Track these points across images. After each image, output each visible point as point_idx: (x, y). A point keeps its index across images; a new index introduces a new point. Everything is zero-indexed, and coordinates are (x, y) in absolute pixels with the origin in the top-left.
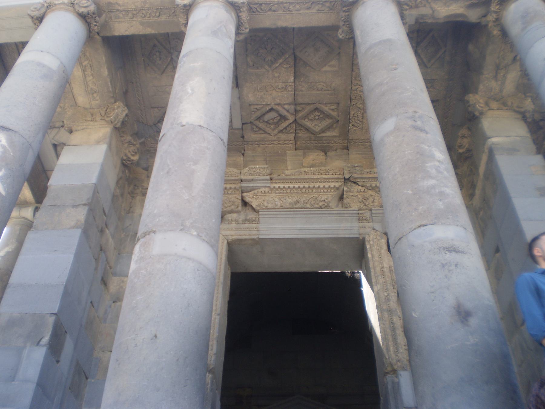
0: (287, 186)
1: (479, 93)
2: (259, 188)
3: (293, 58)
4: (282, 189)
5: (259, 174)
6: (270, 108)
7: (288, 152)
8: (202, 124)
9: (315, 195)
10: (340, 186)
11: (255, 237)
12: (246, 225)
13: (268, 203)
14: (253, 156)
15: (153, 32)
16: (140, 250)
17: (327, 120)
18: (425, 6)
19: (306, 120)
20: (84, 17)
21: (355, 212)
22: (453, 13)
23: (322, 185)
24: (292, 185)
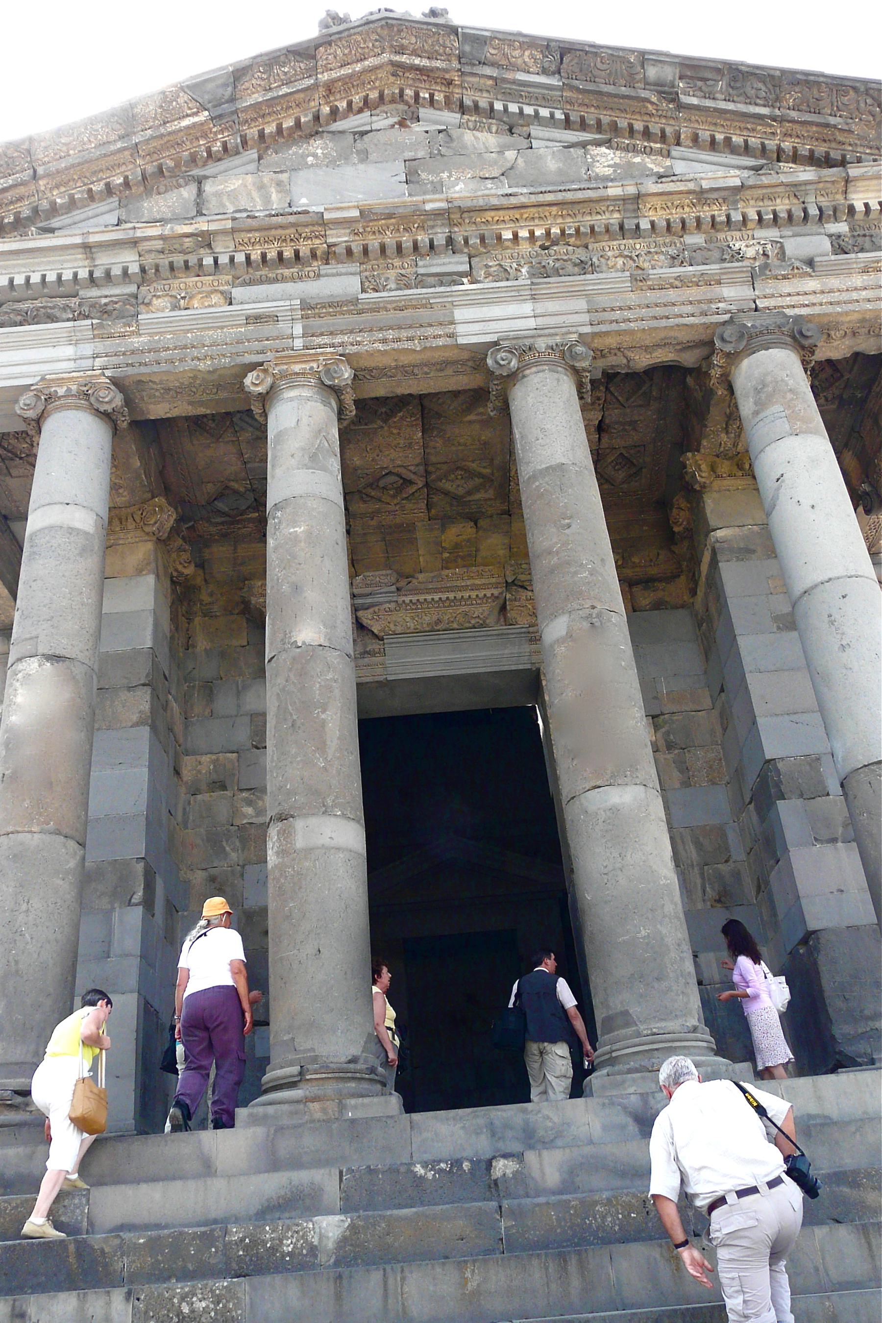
0: (422, 598)
1: (702, 451)
2: (381, 604)
3: (420, 408)
4: (414, 604)
5: (379, 585)
6: (387, 471)
7: (418, 524)
8: (322, 641)
9: (466, 609)
10: (501, 593)
11: (381, 678)
12: (366, 660)
13: (395, 625)
14: (365, 534)
15: (208, 412)
16: (279, 838)
17: (476, 479)
18: (615, 355)
19: (444, 481)
20: (107, 416)
21: (523, 630)
22: (659, 360)
23: (474, 594)
24: (429, 597)
